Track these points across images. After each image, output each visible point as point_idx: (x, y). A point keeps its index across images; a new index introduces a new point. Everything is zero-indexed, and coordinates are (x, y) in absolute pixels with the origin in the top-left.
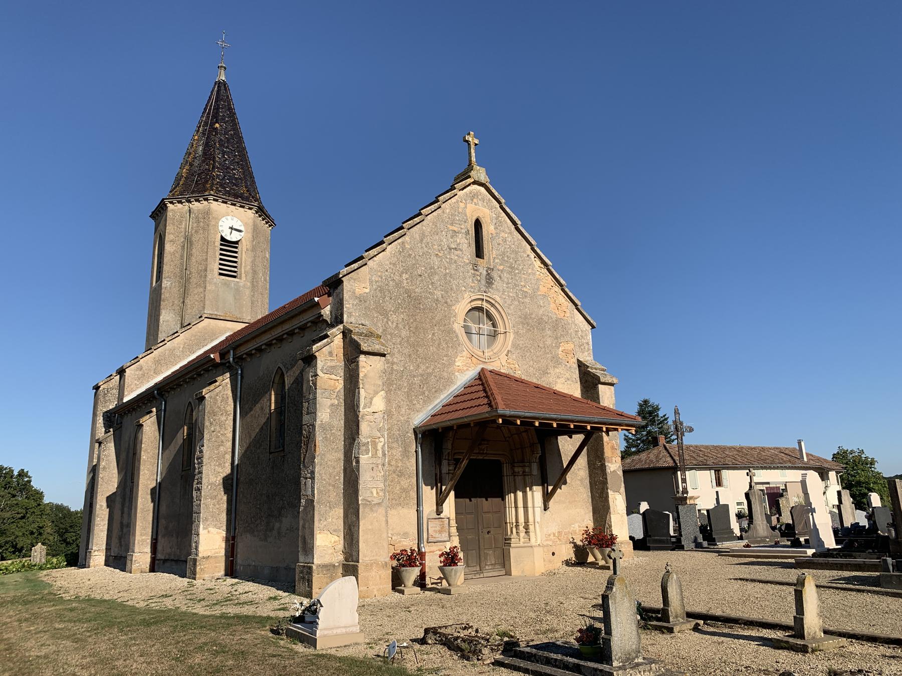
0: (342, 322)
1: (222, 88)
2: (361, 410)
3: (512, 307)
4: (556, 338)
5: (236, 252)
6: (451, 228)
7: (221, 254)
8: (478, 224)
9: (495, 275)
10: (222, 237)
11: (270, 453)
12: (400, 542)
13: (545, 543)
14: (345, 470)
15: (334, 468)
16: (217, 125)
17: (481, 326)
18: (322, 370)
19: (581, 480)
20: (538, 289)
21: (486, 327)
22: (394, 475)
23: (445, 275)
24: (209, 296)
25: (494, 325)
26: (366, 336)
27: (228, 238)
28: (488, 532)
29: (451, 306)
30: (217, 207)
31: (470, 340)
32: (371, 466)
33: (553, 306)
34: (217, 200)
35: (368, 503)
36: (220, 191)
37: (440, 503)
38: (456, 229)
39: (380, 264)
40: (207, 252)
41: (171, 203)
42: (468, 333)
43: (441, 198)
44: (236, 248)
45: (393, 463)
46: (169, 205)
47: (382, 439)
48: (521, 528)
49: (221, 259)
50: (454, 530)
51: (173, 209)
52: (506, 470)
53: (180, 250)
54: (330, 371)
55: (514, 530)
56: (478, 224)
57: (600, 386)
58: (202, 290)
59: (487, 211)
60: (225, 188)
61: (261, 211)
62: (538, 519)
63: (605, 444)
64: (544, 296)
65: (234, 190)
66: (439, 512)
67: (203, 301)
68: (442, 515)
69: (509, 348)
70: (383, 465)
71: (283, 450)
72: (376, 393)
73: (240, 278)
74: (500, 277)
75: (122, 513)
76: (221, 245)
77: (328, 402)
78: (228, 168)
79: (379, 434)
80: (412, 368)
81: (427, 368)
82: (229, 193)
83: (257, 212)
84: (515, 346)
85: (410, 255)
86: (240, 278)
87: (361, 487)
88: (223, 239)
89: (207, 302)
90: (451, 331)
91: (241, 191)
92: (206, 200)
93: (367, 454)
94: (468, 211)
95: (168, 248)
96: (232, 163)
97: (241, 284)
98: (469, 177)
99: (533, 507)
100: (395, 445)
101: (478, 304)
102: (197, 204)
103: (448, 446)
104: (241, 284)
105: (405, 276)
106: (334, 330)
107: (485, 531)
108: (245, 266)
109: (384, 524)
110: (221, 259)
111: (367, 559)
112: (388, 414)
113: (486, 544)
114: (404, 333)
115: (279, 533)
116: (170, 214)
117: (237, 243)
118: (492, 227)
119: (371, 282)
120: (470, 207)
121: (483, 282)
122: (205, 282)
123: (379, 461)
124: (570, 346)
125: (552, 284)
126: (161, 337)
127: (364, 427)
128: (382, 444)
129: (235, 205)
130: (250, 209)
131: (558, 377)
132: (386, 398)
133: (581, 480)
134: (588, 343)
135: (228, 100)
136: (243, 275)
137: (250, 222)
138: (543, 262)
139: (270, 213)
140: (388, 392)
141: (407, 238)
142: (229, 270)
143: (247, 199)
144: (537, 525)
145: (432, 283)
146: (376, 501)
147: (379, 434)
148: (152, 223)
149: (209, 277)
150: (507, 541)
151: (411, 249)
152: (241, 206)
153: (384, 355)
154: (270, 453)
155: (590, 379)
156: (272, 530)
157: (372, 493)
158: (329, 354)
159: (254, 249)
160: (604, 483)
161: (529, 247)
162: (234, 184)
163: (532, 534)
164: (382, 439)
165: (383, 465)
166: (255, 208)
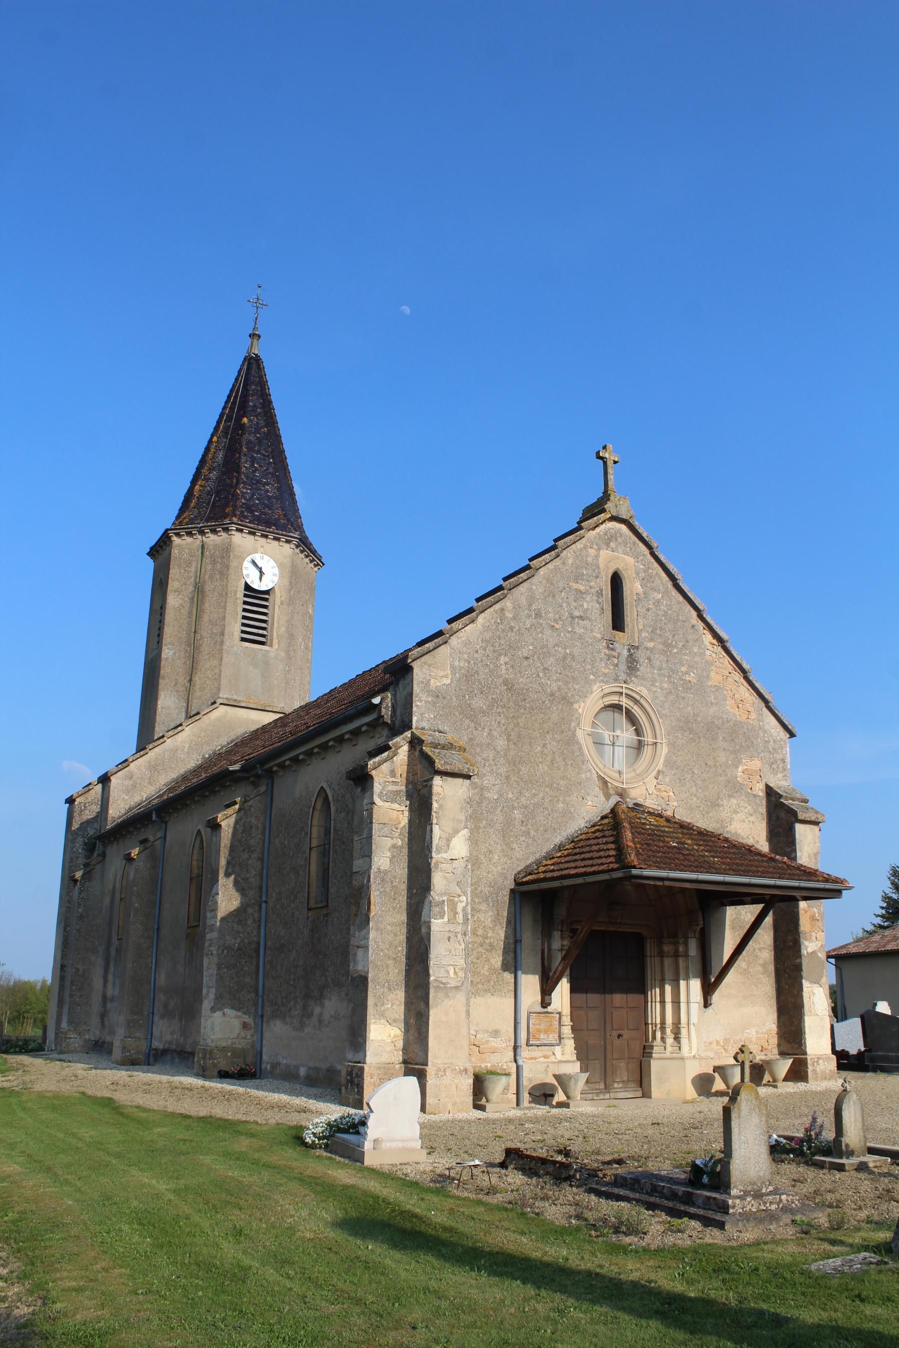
0: (410, 728)
1: (254, 366)
2: (434, 855)
3: (667, 705)
4: (735, 752)
5: (266, 607)
6: (575, 586)
7: (245, 610)
8: (616, 581)
9: (641, 655)
10: (246, 584)
11: (309, 909)
12: (487, 1042)
13: (703, 1055)
14: (409, 939)
15: (395, 935)
16: (245, 420)
17: (618, 733)
18: (380, 796)
19: (763, 965)
20: (708, 677)
21: (626, 735)
22: (480, 949)
23: (564, 658)
24: (226, 672)
25: (638, 732)
26: (443, 748)
27: (256, 585)
28: (619, 1036)
29: (572, 704)
30: (240, 540)
31: (601, 754)
32: (447, 935)
33: (730, 702)
34: (241, 531)
35: (444, 987)
36: (246, 517)
37: (546, 990)
38: (582, 588)
39: (468, 643)
40: (225, 608)
41: (178, 535)
42: (599, 743)
43: (561, 543)
44: (266, 600)
45: (480, 932)
46: (174, 538)
47: (463, 898)
48: (668, 1031)
49: (244, 617)
50: (567, 1031)
51: (182, 544)
52: (650, 949)
53: (187, 605)
54: (391, 797)
55: (658, 1035)
56: (616, 581)
57: (799, 827)
58: (216, 663)
59: (630, 560)
60: (252, 512)
61: (305, 544)
62: (694, 1019)
63: (801, 912)
64: (717, 688)
65: (265, 514)
66: (545, 1004)
67: (218, 679)
68: (549, 1009)
69: (660, 766)
70: (465, 934)
71: (327, 906)
72: (456, 831)
73: (271, 646)
74: (649, 659)
75: (106, 981)
76: (245, 596)
77: (388, 842)
78: (259, 482)
79: (459, 892)
80: (510, 795)
81: (534, 795)
82: (258, 520)
83: (297, 547)
84: (668, 762)
85: (512, 628)
86: (271, 646)
87: (432, 963)
88: (247, 587)
89: (224, 682)
90: (571, 740)
91: (278, 517)
92: (226, 530)
93: (442, 917)
94: (601, 562)
95: (173, 600)
96: (265, 474)
97: (272, 655)
98: (604, 511)
99: (688, 1002)
100: (483, 907)
101: (614, 699)
102: (212, 537)
103: (561, 911)
105: (503, 659)
106: (398, 739)
107: (615, 1033)
108: (279, 628)
109: (464, 1015)
110: (244, 617)
111: (439, 1061)
112: (473, 861)
113: (619, 1054)
114: (501, 743)
115: (320, 1021)
116: (175, 552)
117: (267, 592)
118: (638, 587)
119: (453, 668)
120: (605, 554)
121: (623, 667)
122: (221, 651)
123: (459, 929)
124: (756, 764)
125: (730, 669)
126: (159, 731)
127: (438, 881)
128: (463, 904)
129: (266, 537)
130: (288, 542)
131: (736, 812)
132: (470, 839)
133: (763, 965)
134: (783, 761)
135: (262, 384)
136: (275, 641)
138: (716, 635)
139: (316, 546)
140: (472, 831)
142: (256, 631)
143: (284, 528)
144: (692, 1028)
145: (545, 669)
146: (453, 983)
147: (459, 892)
148: (150, 564)
149: (227, 643)
150: (647, 1051)
151: (514, 618)
152: (276, 539)
153: (468, 777)
154: (309, 909)
155: (783, 815)
156: (310, 1016)
157: (448, 972)
158: (389, 773)
159: (291, 602)
160: (798, 969)
161: (694, 614)
162: (267, 506)
163: (684, 1041)
164: (463, 898)
165: (465, 934)
166: (295, 541)
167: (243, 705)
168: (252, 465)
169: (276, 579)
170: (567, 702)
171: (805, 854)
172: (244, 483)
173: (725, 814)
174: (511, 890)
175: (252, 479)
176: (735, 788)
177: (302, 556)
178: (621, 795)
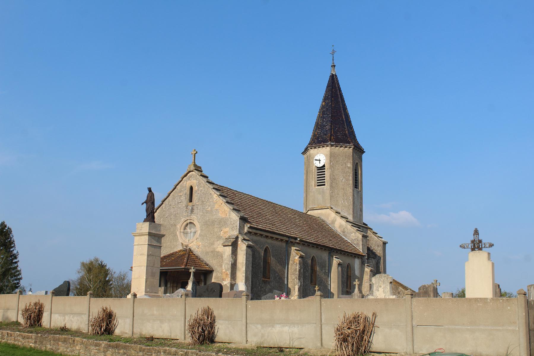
8: (191, 188)
9: (195, 208)
30: (312, 151)
56: (191, 188)
59: (195, 181)
64: (217, 210)
78: (324, 126)
83: (332, 146)
84: (200, 235)
88: (318, 167)
90: (176, 235)
117: (324, 166)
121: (190, 212)
129: (319, 147)
134: (236, 226)
137: (328, 153)
141: (163, 205)
159: (331, 167)
162: (325, 135)
169: (325, 161)
170: (175, 225)
171: (226, 255)
172: (319, 128)
173: (215, 246)
174: (211, 272)
176: (219, 238)
177: (337, 148)
178: (186, 247)
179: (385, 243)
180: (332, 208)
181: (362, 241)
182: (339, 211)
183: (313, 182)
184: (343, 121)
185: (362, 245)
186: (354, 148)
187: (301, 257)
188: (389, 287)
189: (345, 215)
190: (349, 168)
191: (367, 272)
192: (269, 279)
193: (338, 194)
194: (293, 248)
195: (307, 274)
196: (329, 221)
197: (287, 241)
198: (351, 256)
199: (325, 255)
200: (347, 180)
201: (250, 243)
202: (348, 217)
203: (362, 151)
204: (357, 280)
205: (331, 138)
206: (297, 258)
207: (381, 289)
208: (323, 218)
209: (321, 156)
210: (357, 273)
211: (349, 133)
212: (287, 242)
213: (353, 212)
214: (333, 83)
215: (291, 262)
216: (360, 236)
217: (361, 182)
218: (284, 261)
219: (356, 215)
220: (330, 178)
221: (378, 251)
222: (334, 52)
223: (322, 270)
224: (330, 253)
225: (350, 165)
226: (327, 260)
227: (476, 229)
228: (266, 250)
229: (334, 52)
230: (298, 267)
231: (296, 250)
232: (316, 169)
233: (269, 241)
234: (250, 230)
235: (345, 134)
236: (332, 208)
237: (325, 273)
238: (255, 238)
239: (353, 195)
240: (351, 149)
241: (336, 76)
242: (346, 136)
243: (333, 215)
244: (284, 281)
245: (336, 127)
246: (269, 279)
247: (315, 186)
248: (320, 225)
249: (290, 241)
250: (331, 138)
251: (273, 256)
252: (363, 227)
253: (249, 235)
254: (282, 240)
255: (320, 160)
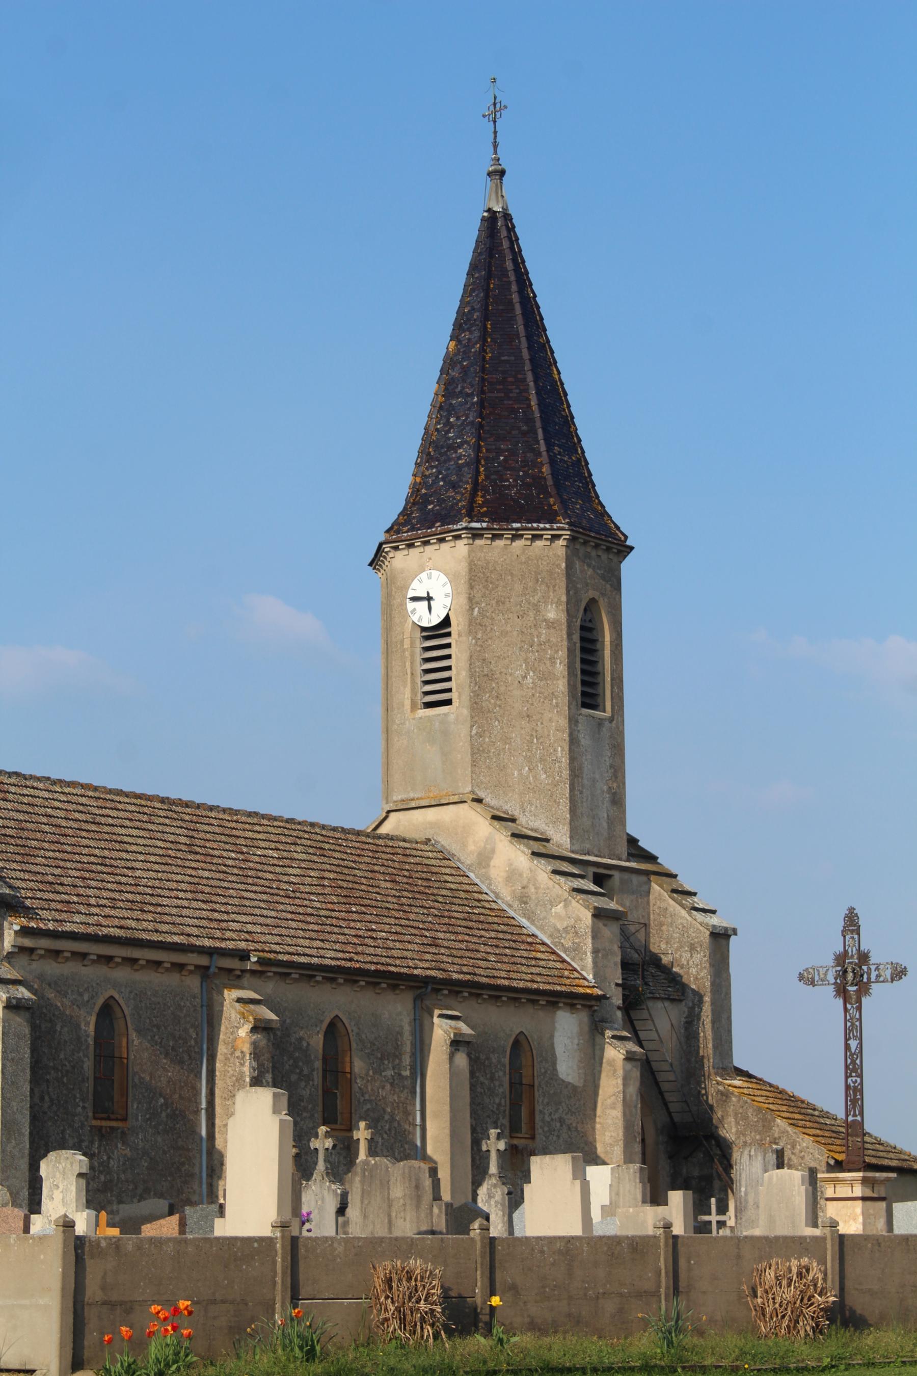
27: (425, 624)
30: (400, 560)
34: (396, 548)
76: (427, 638)
83: (476, 535)
88: (424, 629)
104: (452, 717)
108: (458, 674)
129: (427, 543)
137: (463, 568)
159: (474, 625)
162: (454, 486)
167: (413, 805)
168: (448, 423)
169: (448, 602)
175: (442, 447)
177: (499, 543)
179: (721, 938)
180: (479, 801)
181: (593, 938)
182: (511, 807)
183: (407, 692)
184: (529, 420)
185: (595, 951)
186: (573, 540)
187: (260, 1027)
188: (73, 1188)
189: (532, 821)
190: (551, 625)
191: (611, 1063)
192: (124, 1119)
193: (506, 740)
194: (230, 995)
195: (306, 1093)
196: (466, 856)
197: (203, 971)
198: (534, 1002)
199: (396, 1009)
200: (546, 677)
201: (23, 993)
202: (550, 832)
203: (620, 548)
204: (362, 1124)
205: (472, 501)
206: (243, 1032)
207: (58, 1195)
208: (444, 841)
209: (434, 581)
210: (567, 1068)
211: (554, 474)
212: (203, 971)
213: (573, 810)
214: (491, 256)
215: (222, 1050)
216: (587, 917)
217: (618, 681)
218: (194, 1044)
219: (586, 822)
220: (472, 675)
221: (694, 968)
222: (496, 110)
223: (378, 1071)
224: (418, 999)
225: (554, 612)
226: (407, 1029)
227: (851, 910)
228: (107, 1012)
229: (496, 110)
230: (246, 1069)
231: (239, 1000)
232: (418, 634)
233: (122, 974)
234: (27, 942)
235: (538, 480)
236: (479, 801)
237: (397, 1082)
238: (52, 968)
239: (573, 741)
240: (561, 542)
241: (507, 217)
242: (543, 489)
243: (481, 828)
244: (193, 1130)
245: (499, 452)
246: (124, 1119)
247: (414, 707)
248: (419, 877)
249: (220, 967)
250: (472, 501)
251: (139, 1031)
252: (616, 871)
253: (23, 960)
254: (180, 967)
255: (429, 599)
